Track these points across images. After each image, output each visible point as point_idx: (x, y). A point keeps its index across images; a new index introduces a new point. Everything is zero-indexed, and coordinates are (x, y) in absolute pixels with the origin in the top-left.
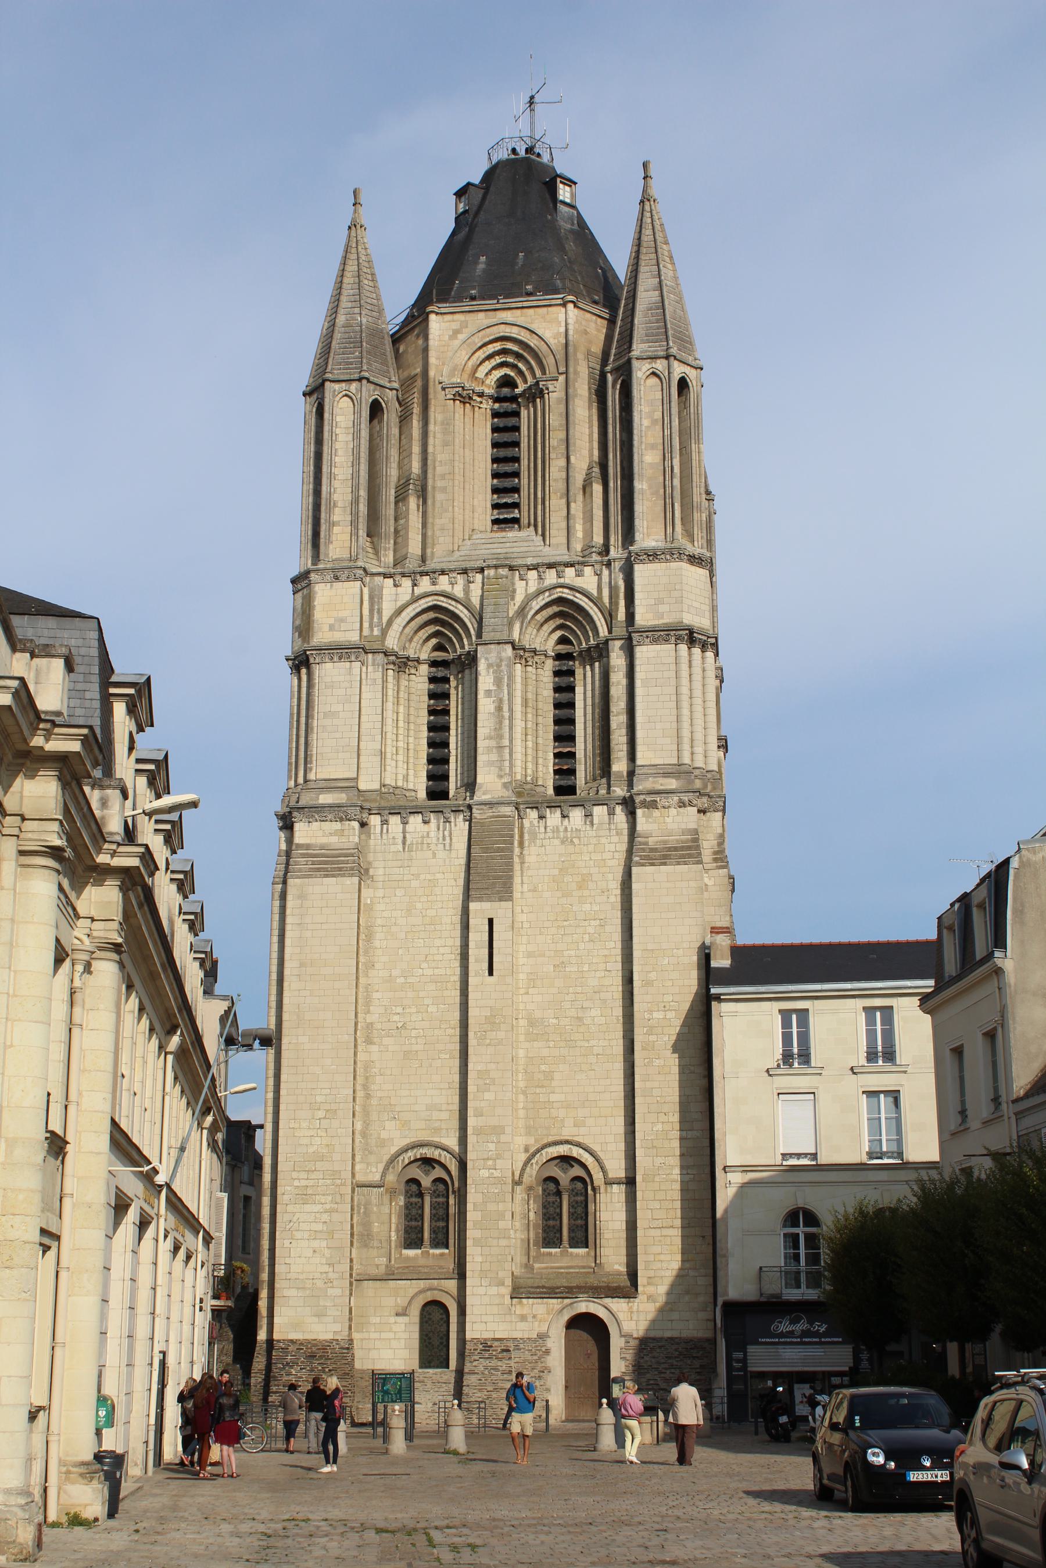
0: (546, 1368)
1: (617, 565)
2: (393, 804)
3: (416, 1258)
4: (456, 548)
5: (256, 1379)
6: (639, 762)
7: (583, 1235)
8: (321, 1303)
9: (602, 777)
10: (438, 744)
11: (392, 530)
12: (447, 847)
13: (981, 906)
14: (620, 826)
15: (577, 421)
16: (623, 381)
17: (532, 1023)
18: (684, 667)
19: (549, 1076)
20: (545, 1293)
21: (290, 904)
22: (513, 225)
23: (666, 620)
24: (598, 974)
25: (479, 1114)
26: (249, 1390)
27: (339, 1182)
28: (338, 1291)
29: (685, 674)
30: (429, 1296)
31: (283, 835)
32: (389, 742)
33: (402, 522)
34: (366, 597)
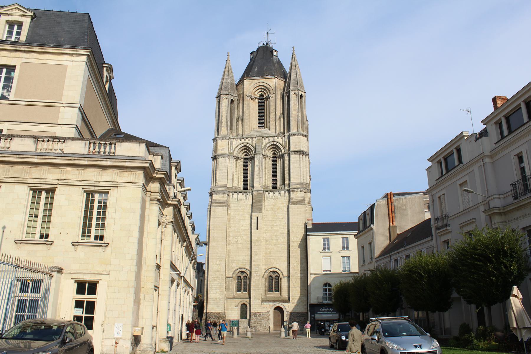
1: (286, 137)
5: (203, 321)
7: (278, 289)
13: (368, 214)
17: (266, 241)
18: (302, 160)
22: (263, 60)
29: (302, 161)
30: (243, 303)
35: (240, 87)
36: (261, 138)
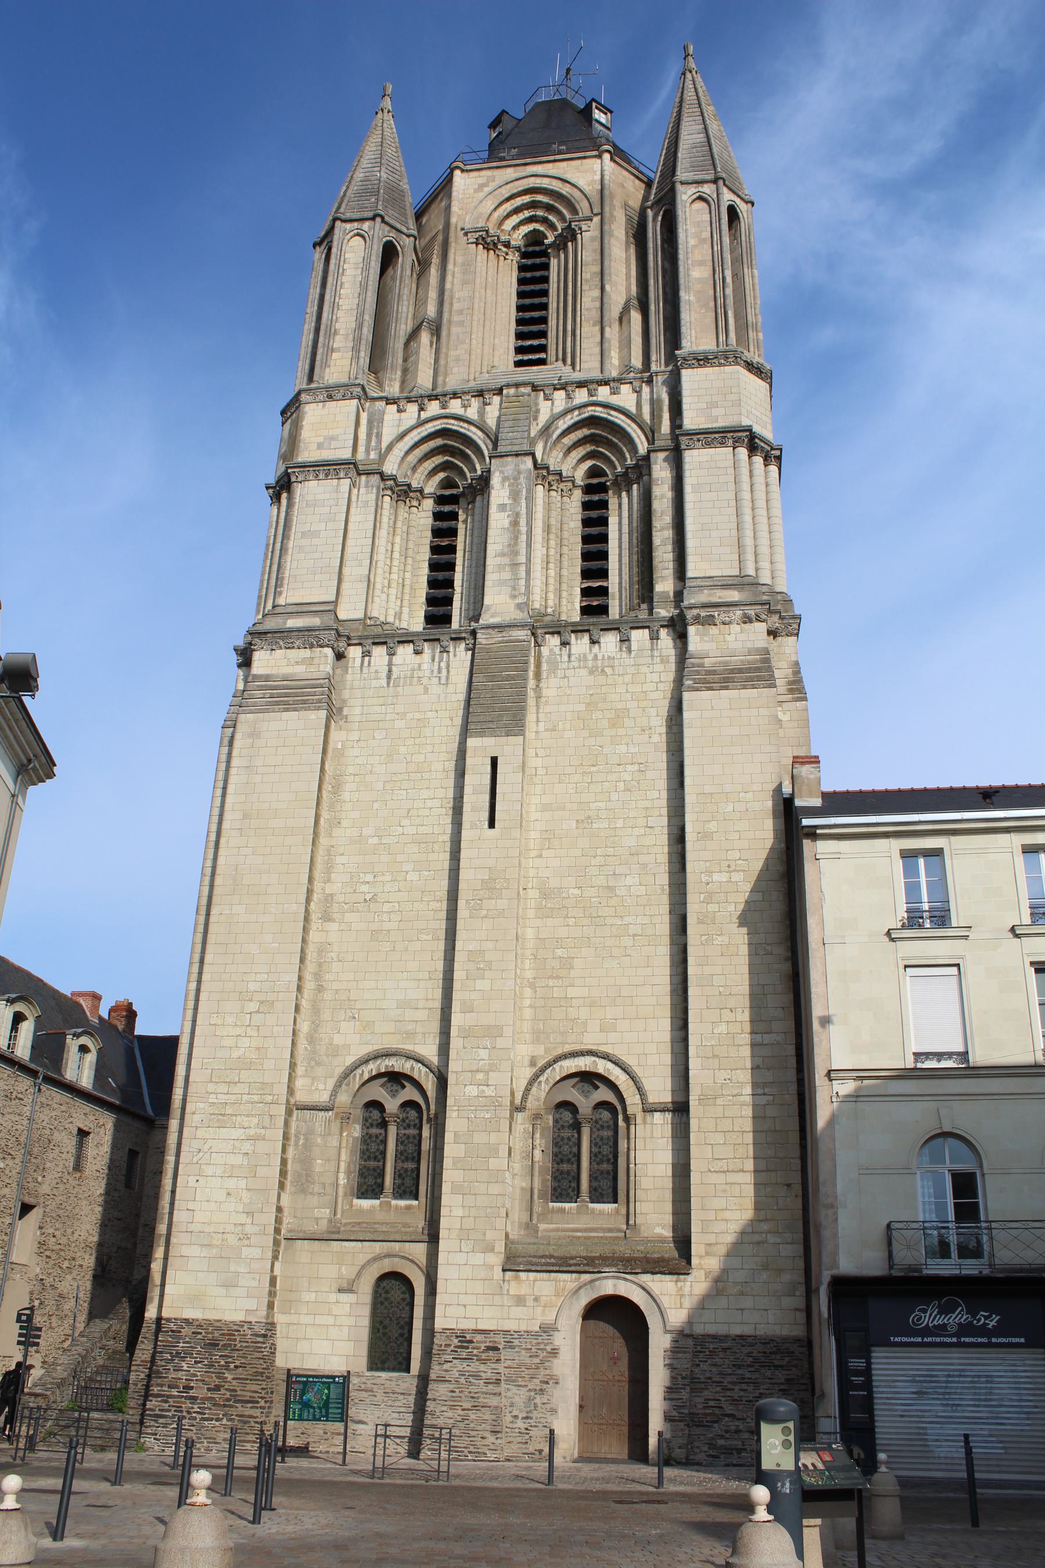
0: (552, 1377)
3: (372, 1210)
6: (690, 574)
7: (610, 1184)
8: (232, 1269)
12: (443, 681)
14: (664, 653)
17: (546, 894)
18: (745, 471)
19: (567, 963)
20: (553, 1265)
21: (237, 744)
24: (636, 832)
25: (468, 1009)
26: (127, 1389)
27: (269, 1098)
28: (258, 1251)
30: (387, 1266)
31: (241, 673)
32: (380, 571)
36: (527, 390)
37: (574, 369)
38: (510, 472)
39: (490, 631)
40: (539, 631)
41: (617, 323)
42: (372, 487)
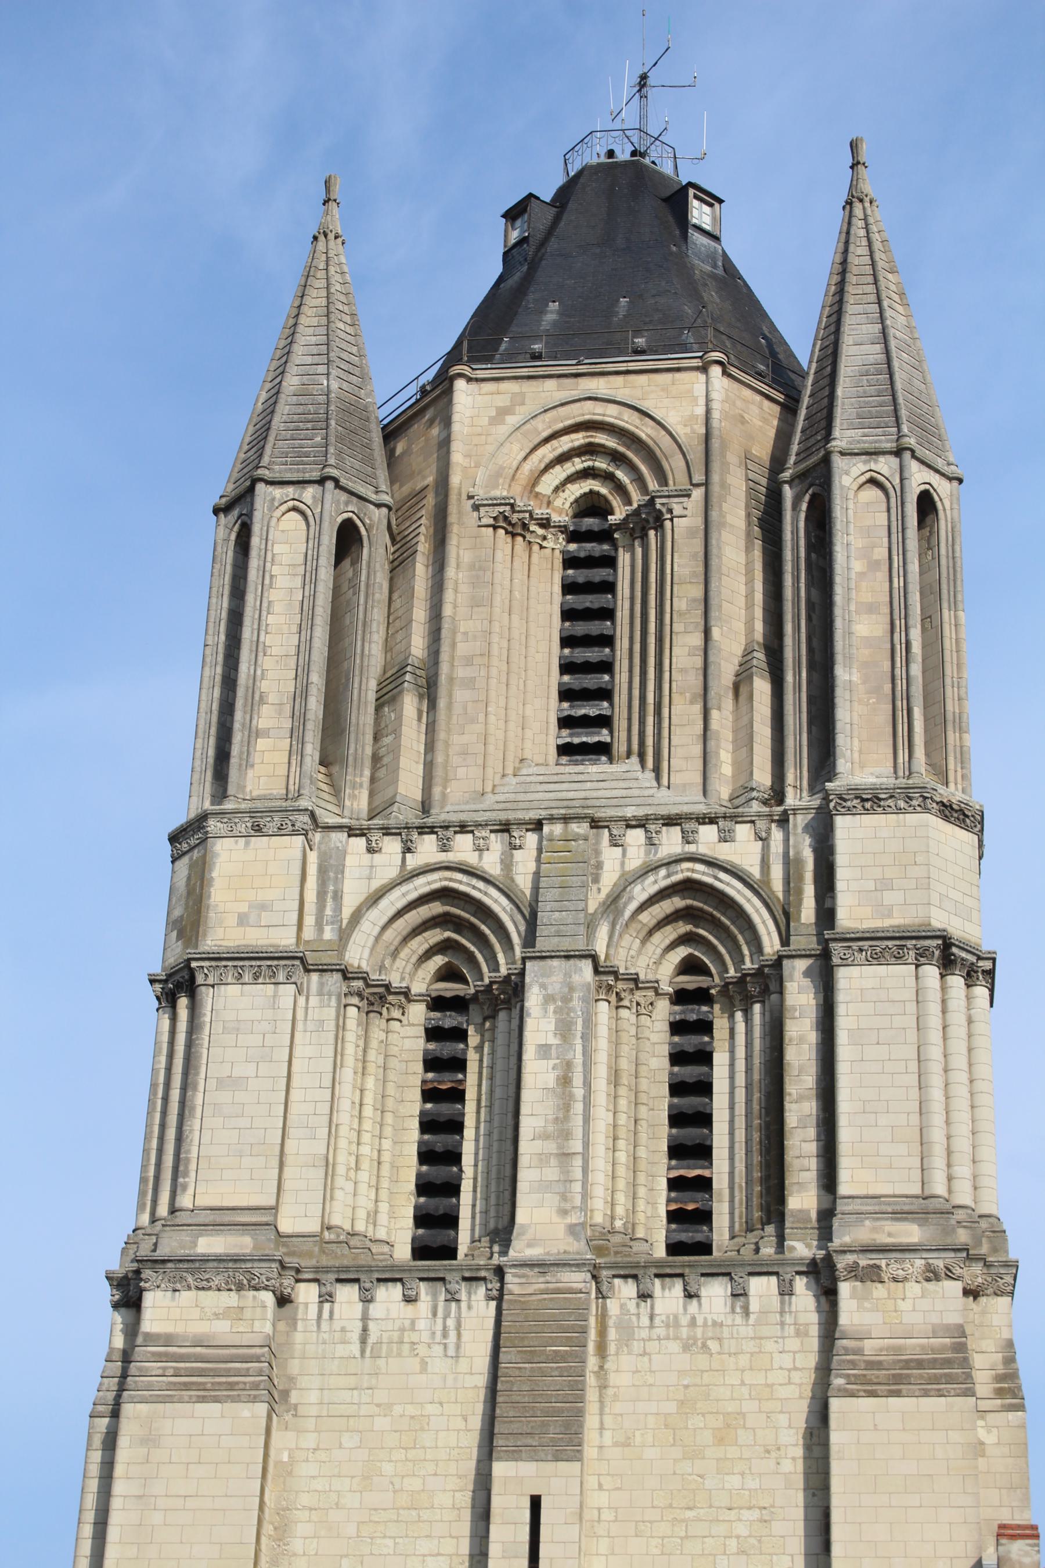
1: (799, 821)
2: (346, 1262)
4: (489, 789)
6: (843, 1189)
9: (764, 1223)
10: (439, 1157)
11: (369, 751)
12: (451, 1352)
14: (803, 1319)
15: (724, 570)
16: (813, 496)
18: (934, 1008)
22: (606, 257)
23: (898, 920)
29: (934, 1020)
31: (118, 1319)
32: (343, 1143)
33: (387, 740)
34: (312, 870)
35: (415, 445)
36: (580, 828)
37: (658, 778)
38: (557, 986)
39: (526, 1271)
40: (604, 1273)
41: (731, 695)
42: (330, 995)
